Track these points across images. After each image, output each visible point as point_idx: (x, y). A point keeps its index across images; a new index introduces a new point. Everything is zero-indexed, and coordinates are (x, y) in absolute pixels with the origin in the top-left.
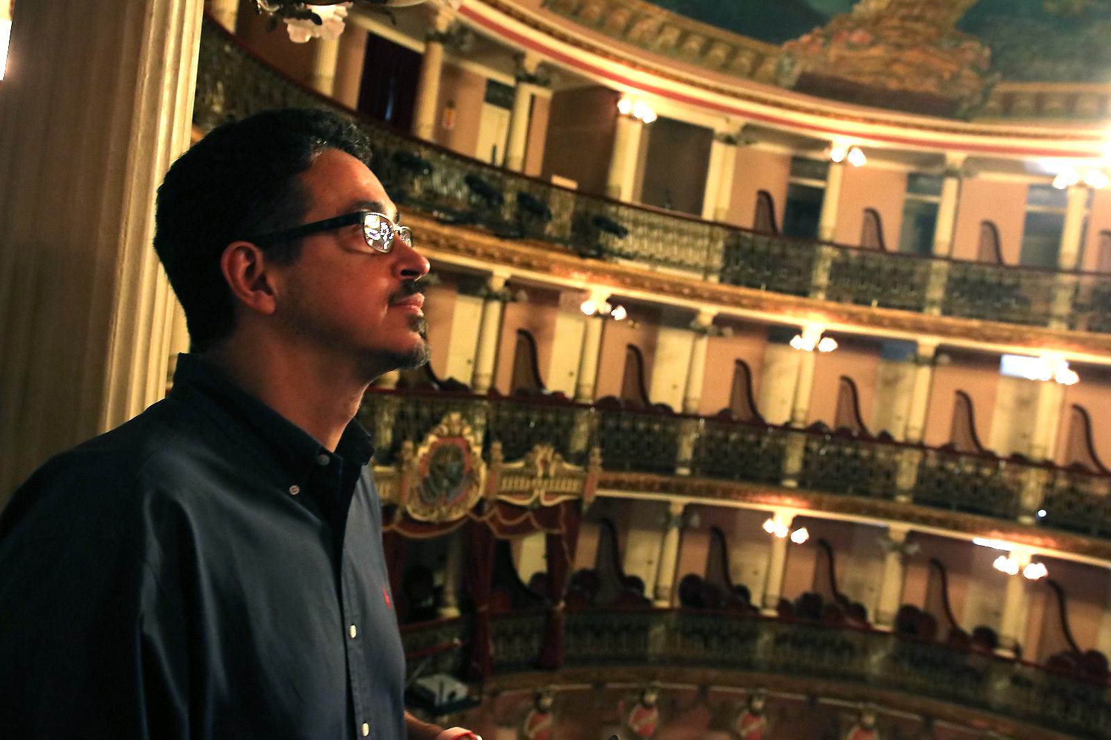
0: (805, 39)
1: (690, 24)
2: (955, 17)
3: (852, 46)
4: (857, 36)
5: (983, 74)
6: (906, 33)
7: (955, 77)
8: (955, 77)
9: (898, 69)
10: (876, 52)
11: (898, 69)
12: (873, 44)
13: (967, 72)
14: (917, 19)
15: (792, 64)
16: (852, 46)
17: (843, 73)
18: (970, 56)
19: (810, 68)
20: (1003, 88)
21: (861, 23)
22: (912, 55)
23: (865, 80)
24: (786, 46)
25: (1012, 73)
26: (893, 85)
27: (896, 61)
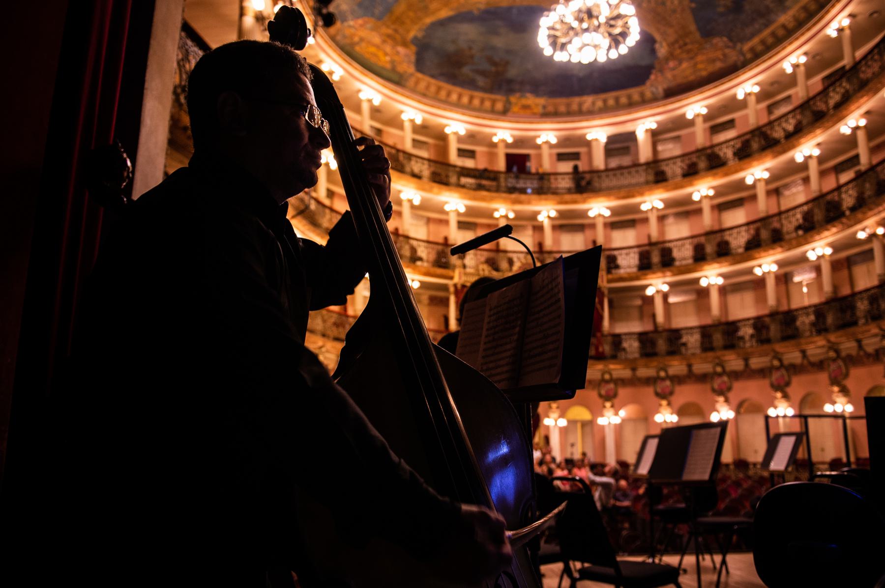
0: (652, 77)
1: (603, 96)
2: (697, 35)
3: (673, 69)
4: (671, 64)
5: (734, 48)
6: (688, 52)
7: (725, 55)
8: (725, 55)
9: (700, 66)
10: (685, 65)
11: (700, 66)
12: (680, 63)
13: (727, 51)
14: (685, 44)
15: (657, 88)
16: (673, 69)
17: (680, 80)
18: (721, 44)
19: (665, 86)
20: (746, 47)
21: (667, 59)
22: (700, 58)
23: (692, 78)
24: (648, 83)
25: (744, 39)
26: (704, 73)
27: (695, 65)
